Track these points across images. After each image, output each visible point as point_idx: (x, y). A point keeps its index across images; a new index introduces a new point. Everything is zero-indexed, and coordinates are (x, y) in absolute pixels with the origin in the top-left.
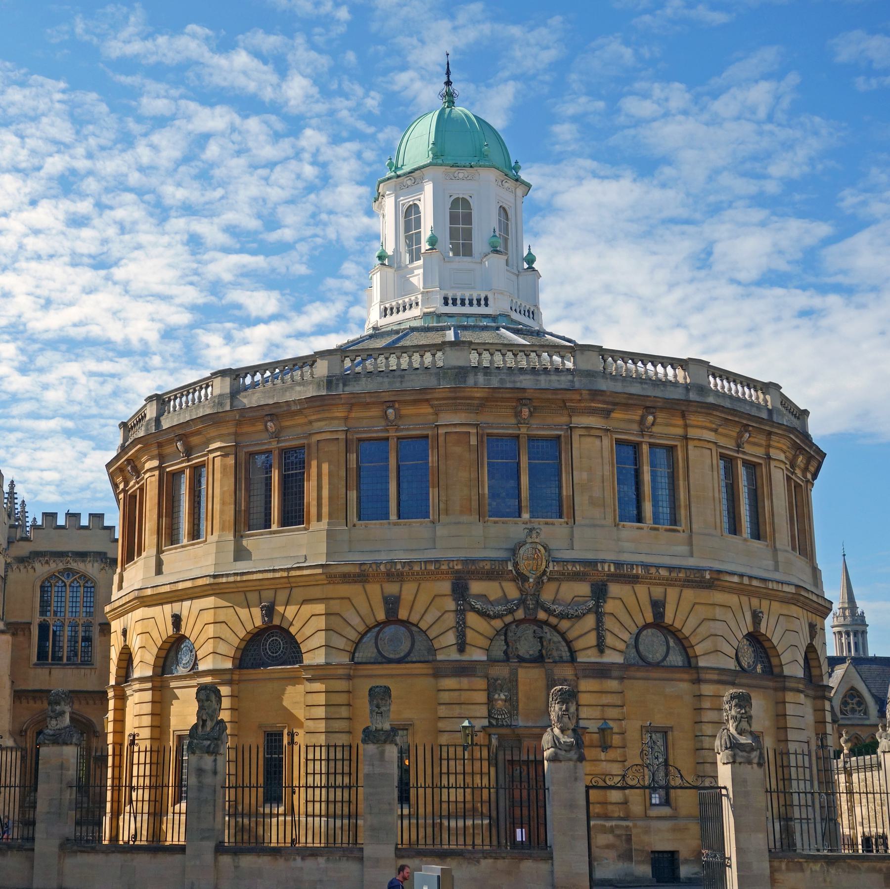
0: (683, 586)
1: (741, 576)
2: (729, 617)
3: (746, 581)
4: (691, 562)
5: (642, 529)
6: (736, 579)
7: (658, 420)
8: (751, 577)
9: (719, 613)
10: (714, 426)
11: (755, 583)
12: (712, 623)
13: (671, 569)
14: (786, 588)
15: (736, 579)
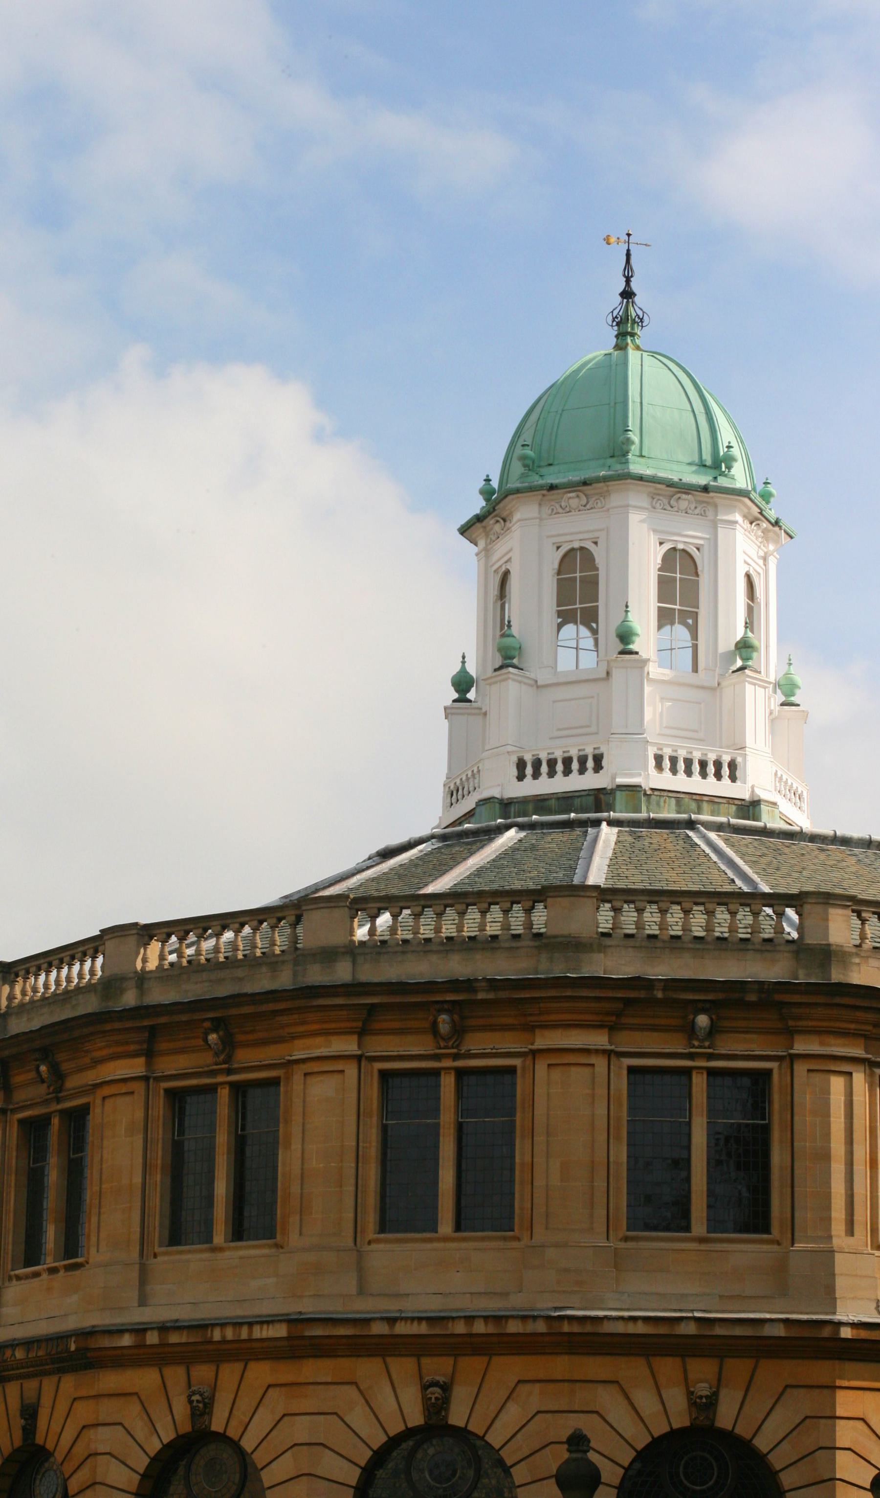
0: (62, 1371)
1: (140, 1331)
2: (132, 1413)
3: (152, 1338)
4: (72, 1323)
5: (37, 1275)
6: (127, 1340)
7: (65, 1067)
8: (163, 1328)
9: (107, 1410)
10: (133, 1047)
11: (174, 1338)
12: (91, 1433)
13: (28, 1343)
14: (259, 1333)
15: (127, 1340)
